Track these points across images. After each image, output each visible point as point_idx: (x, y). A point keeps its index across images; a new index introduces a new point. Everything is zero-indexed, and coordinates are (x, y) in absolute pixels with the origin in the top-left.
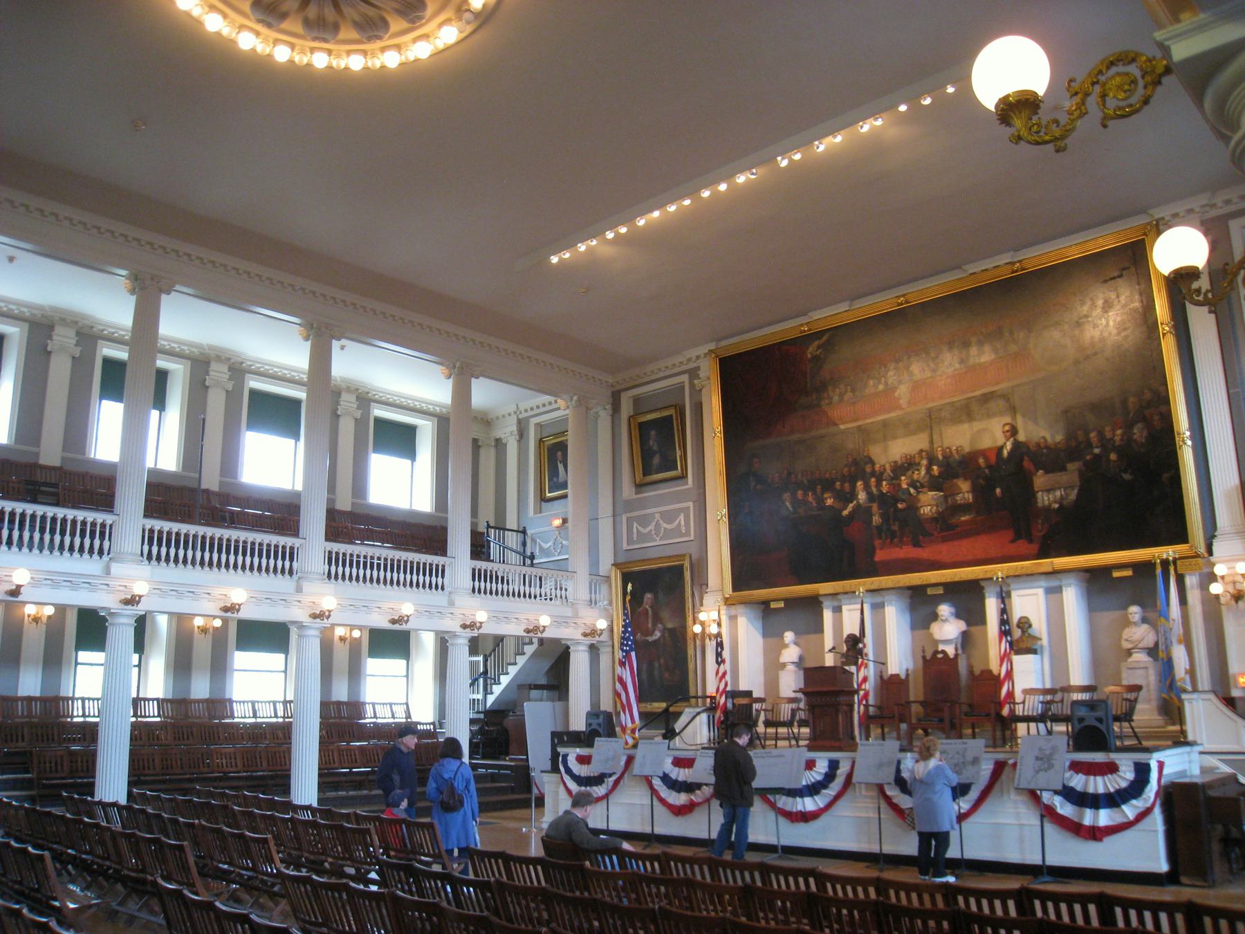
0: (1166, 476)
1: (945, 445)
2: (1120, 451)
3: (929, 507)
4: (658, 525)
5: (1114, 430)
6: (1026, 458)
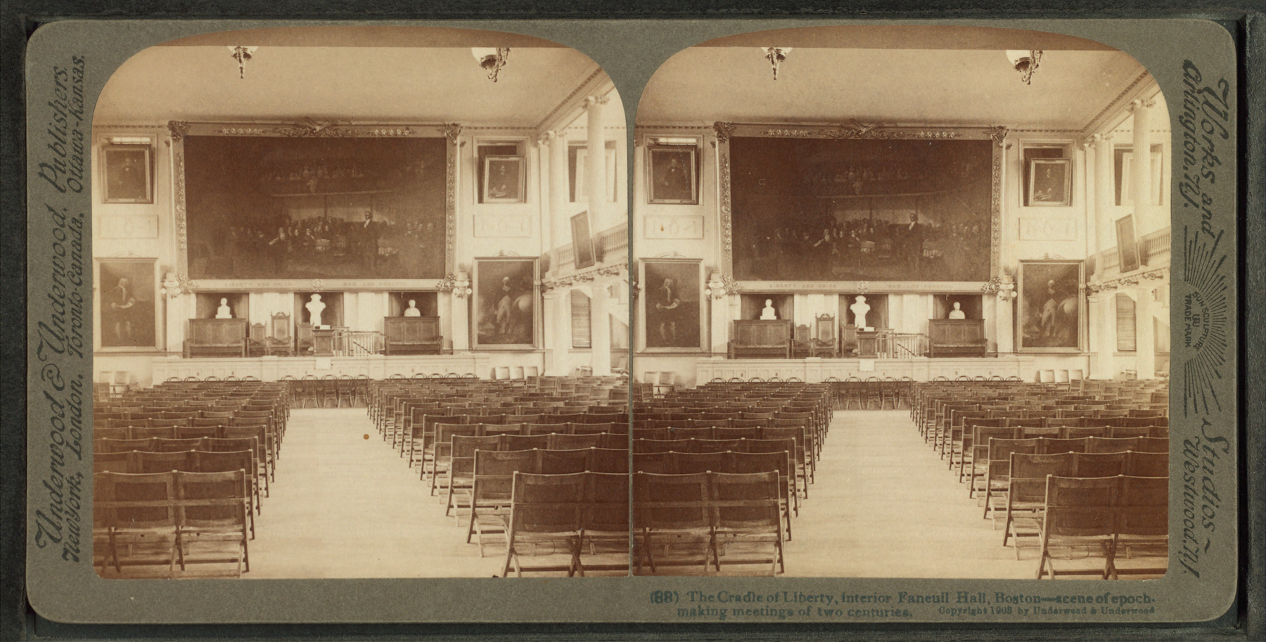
1: (333, 216)
5: (418, 224)
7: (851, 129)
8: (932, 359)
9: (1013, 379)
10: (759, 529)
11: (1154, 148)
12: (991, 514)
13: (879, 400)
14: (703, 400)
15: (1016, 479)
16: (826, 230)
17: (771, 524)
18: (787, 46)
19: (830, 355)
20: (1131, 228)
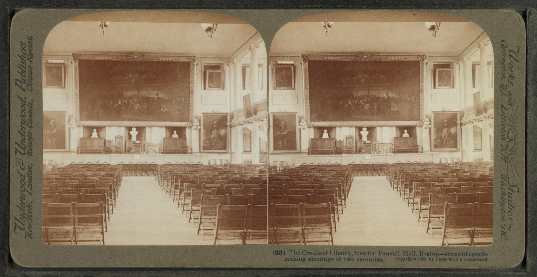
7: (130, 56)
8: (165, 155)
9: (199, 163)
10: (94, 227)
11: (260, 65)
12: (192, 221)
13: (142, 172)
14: (68, 172)
15: (204, 206)
16: (119, 100)
17: (100, 225)
18: (109, 21)
19: (121, 153)
20: (249, 100)
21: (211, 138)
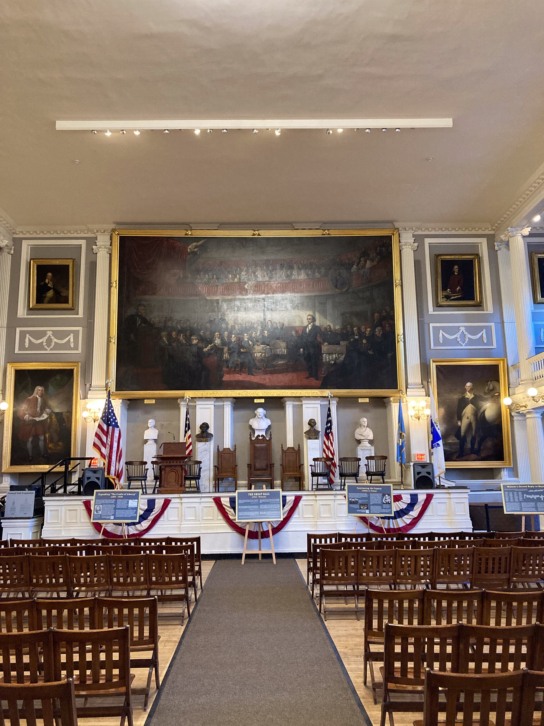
0: (389, 355)
2: (367, 338)
3: (260, 354)
4: (49, 341)
5: (366, 329)
6: (318, 335)
21: (460, 427)
